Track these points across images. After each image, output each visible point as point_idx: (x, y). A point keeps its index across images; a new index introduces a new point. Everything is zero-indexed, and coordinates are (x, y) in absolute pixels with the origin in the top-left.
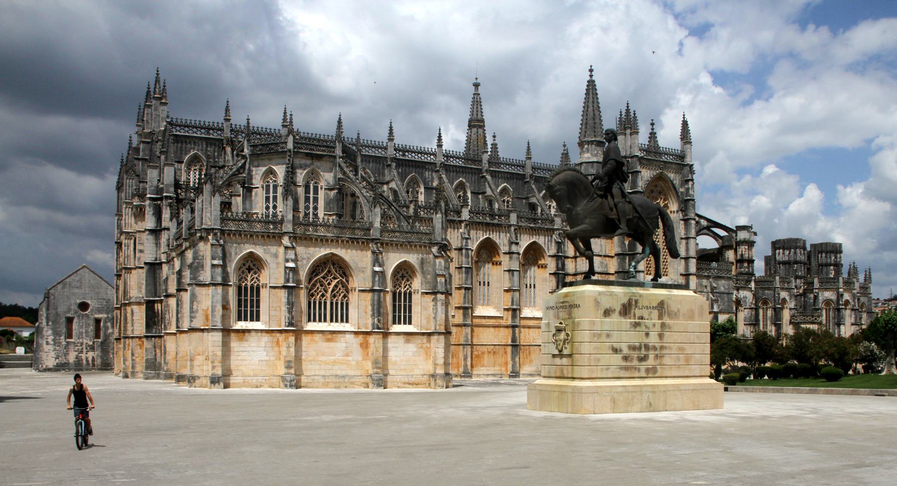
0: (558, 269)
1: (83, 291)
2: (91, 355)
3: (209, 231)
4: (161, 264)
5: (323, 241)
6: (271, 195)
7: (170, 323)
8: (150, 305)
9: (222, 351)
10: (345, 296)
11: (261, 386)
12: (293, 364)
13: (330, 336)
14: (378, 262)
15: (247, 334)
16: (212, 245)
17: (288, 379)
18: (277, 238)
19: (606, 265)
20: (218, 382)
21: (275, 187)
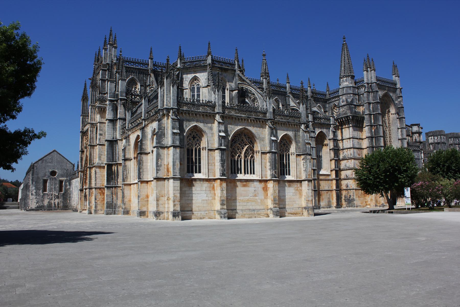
0: (334, 147)
1: (53, 164)
2: (57, 201)
3: (168, 110)
4: (116, 141)
6: (196, 94)
7: (127, 177)
8: (110, 166)
10: (252, 157)
11: (203, 218)
12: (225, 202)
13: (245, 183)
14: (273, 134)
17: (223, 212)
19: (360, 144)
20: (178, 216)
21: (198, 89)
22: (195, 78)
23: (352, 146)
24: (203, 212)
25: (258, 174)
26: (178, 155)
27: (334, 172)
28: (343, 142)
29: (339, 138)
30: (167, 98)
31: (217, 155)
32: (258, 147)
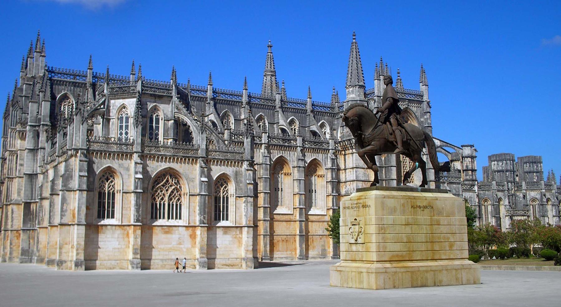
3: (77, 150)
5: (163, 158)
6: (124, 124)
7: (43, 220)
8: (27, 205)
9: (85, 241)
10: (179, 200)
11: (114, 268)
12: (139, 251)
15: (104, 227)
16: (80, 161)
17: (135, 262)
18: (128, 155)
20: (81, 265)
21: (127, 118)
22: (124, 107)
23: (355, 178)
24: (114, 262)
25: (185, 219)
26: (84, 200)
27: (331, 212)
28: (346, 173)
29: (342, 167)
30: (76, 137)
31: (132, 198)
32: (185, 188)
